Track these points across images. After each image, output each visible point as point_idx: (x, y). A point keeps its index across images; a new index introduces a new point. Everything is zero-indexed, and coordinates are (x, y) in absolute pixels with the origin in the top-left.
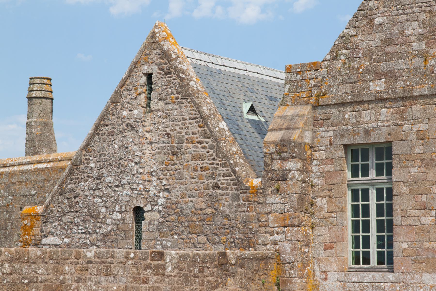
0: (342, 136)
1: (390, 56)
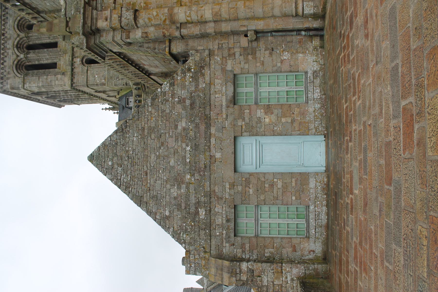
0: (229, 237)
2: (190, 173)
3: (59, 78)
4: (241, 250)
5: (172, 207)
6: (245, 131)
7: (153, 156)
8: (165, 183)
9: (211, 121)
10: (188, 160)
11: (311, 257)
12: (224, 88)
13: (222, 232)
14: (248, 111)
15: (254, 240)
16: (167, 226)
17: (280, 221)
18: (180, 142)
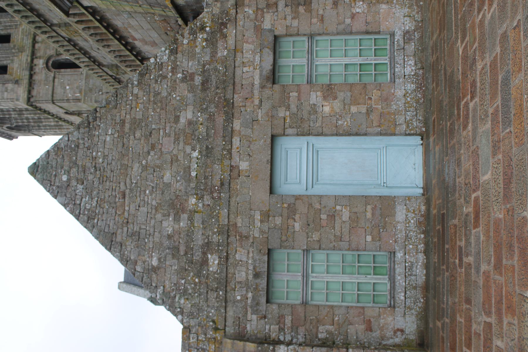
0: (258, 304)
1: (189, 249)
2: (197, 194)
3: (9, 88)
4: (278, 326)
5: (163, 251)
6: (290, 127)
7: (136, 166)
8: (154, 211)
9: (235, 111)
10: (194, 174)
11: (398, 340)
12: (257, 58)
13: (245, 295)
14: (296, 94)
15: (300, 310)
16: (154, 285)
17: (346, 278)
18: (181, 144)
